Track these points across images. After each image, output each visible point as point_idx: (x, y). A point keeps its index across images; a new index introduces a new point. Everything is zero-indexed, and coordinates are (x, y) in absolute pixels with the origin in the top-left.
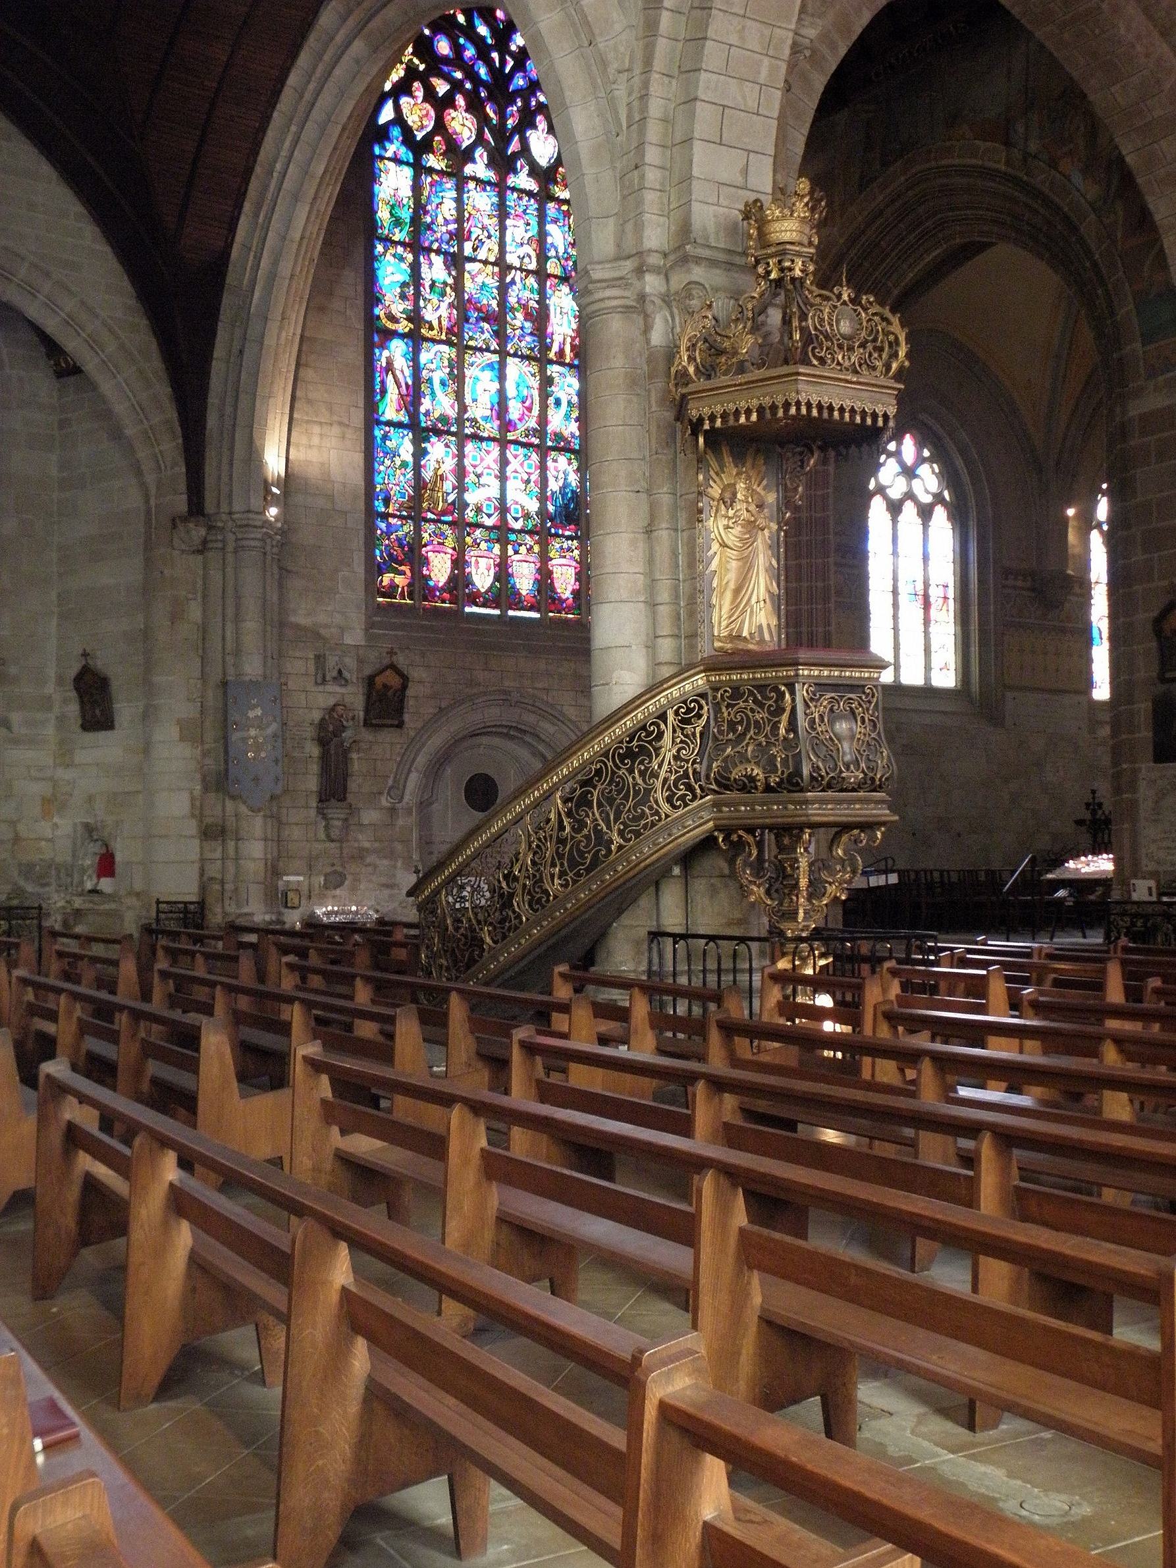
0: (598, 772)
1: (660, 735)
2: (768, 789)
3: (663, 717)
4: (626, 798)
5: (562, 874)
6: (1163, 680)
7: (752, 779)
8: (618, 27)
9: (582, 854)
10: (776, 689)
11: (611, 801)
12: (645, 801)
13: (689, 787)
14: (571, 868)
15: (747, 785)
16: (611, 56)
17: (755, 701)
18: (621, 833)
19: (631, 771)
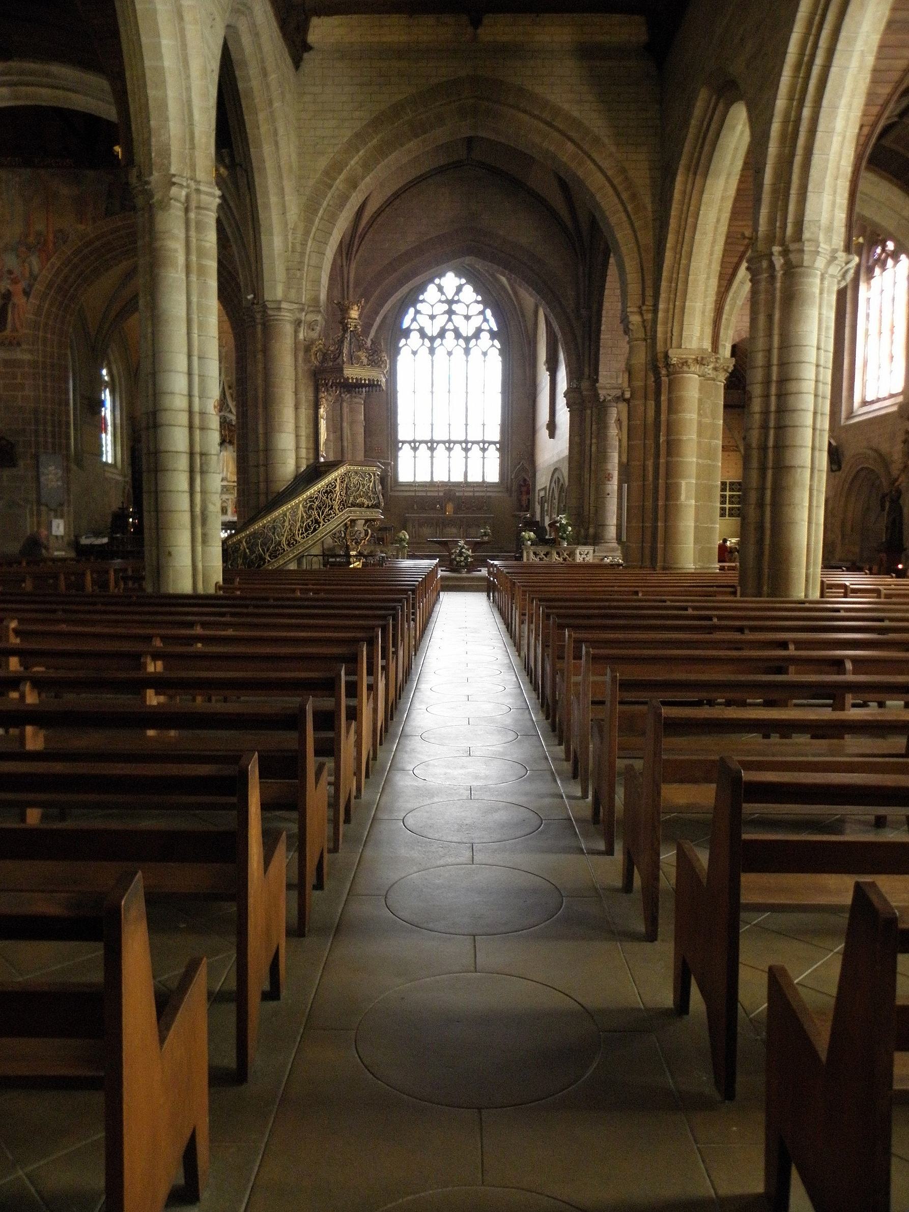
0: (316, 498)
1: (335, 487)
2: (368, 507)
3: (336, 480)
4: (326, 507)
5: (302, 534)
7: (364, 504)
8: (292, 212)
9: (310, 527)
10: (369, 474)
11: (320, 508)
12: (332, 508)
13: (344, 505)
14: (306, 532)
15: (361, 505)
16: (289, 222)
17: (362, 477)
18: (324, 519)
19: (327, 498)
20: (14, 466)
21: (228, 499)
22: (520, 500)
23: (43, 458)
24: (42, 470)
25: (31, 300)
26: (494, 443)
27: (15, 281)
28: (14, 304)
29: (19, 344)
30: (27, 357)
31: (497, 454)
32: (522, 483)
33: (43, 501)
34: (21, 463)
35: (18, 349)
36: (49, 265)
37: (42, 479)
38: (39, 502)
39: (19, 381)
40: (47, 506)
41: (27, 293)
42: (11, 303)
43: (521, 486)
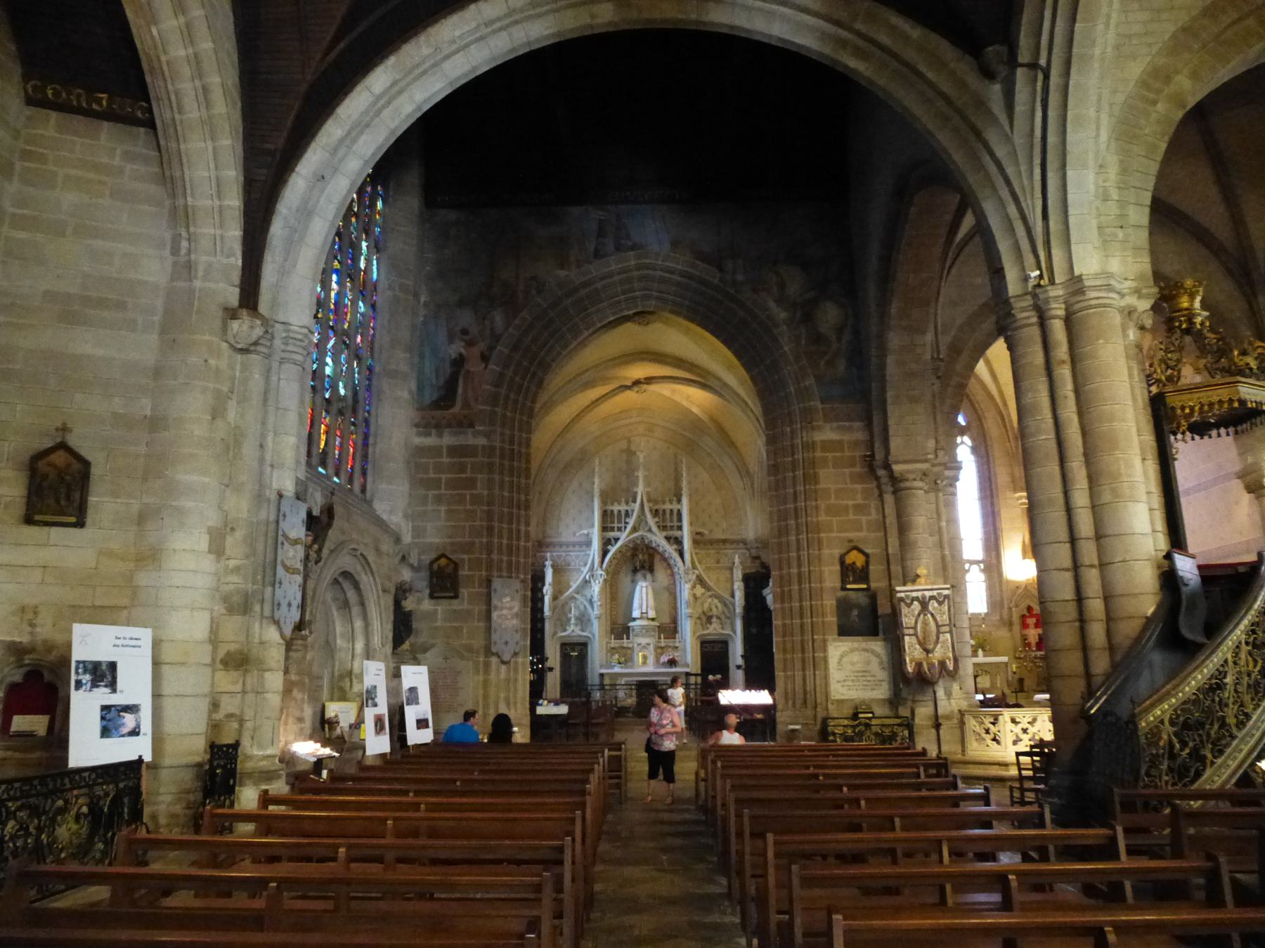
6: (843, 589)
20: (456, 597)
21: (649, 644)
22: (1024, 638)
23: (497, 583)
24: (495, 602)
25: (492, 366)
26: (977, 562)
27: (470, 344)
28: (468, 372)
29: (471, 425)
30: (482, 441)
31: (982, 577)
32: (1025, 612)
33: (494, 650)
34: (464, 592)
35: (470, 430)
36: (517, 322)
37: (495, 615)
38: (488, 652)
39: (468, 475)
40: (499, 657)
41: (485, 358)
42: (463, 372)
43: (1023, 616)
